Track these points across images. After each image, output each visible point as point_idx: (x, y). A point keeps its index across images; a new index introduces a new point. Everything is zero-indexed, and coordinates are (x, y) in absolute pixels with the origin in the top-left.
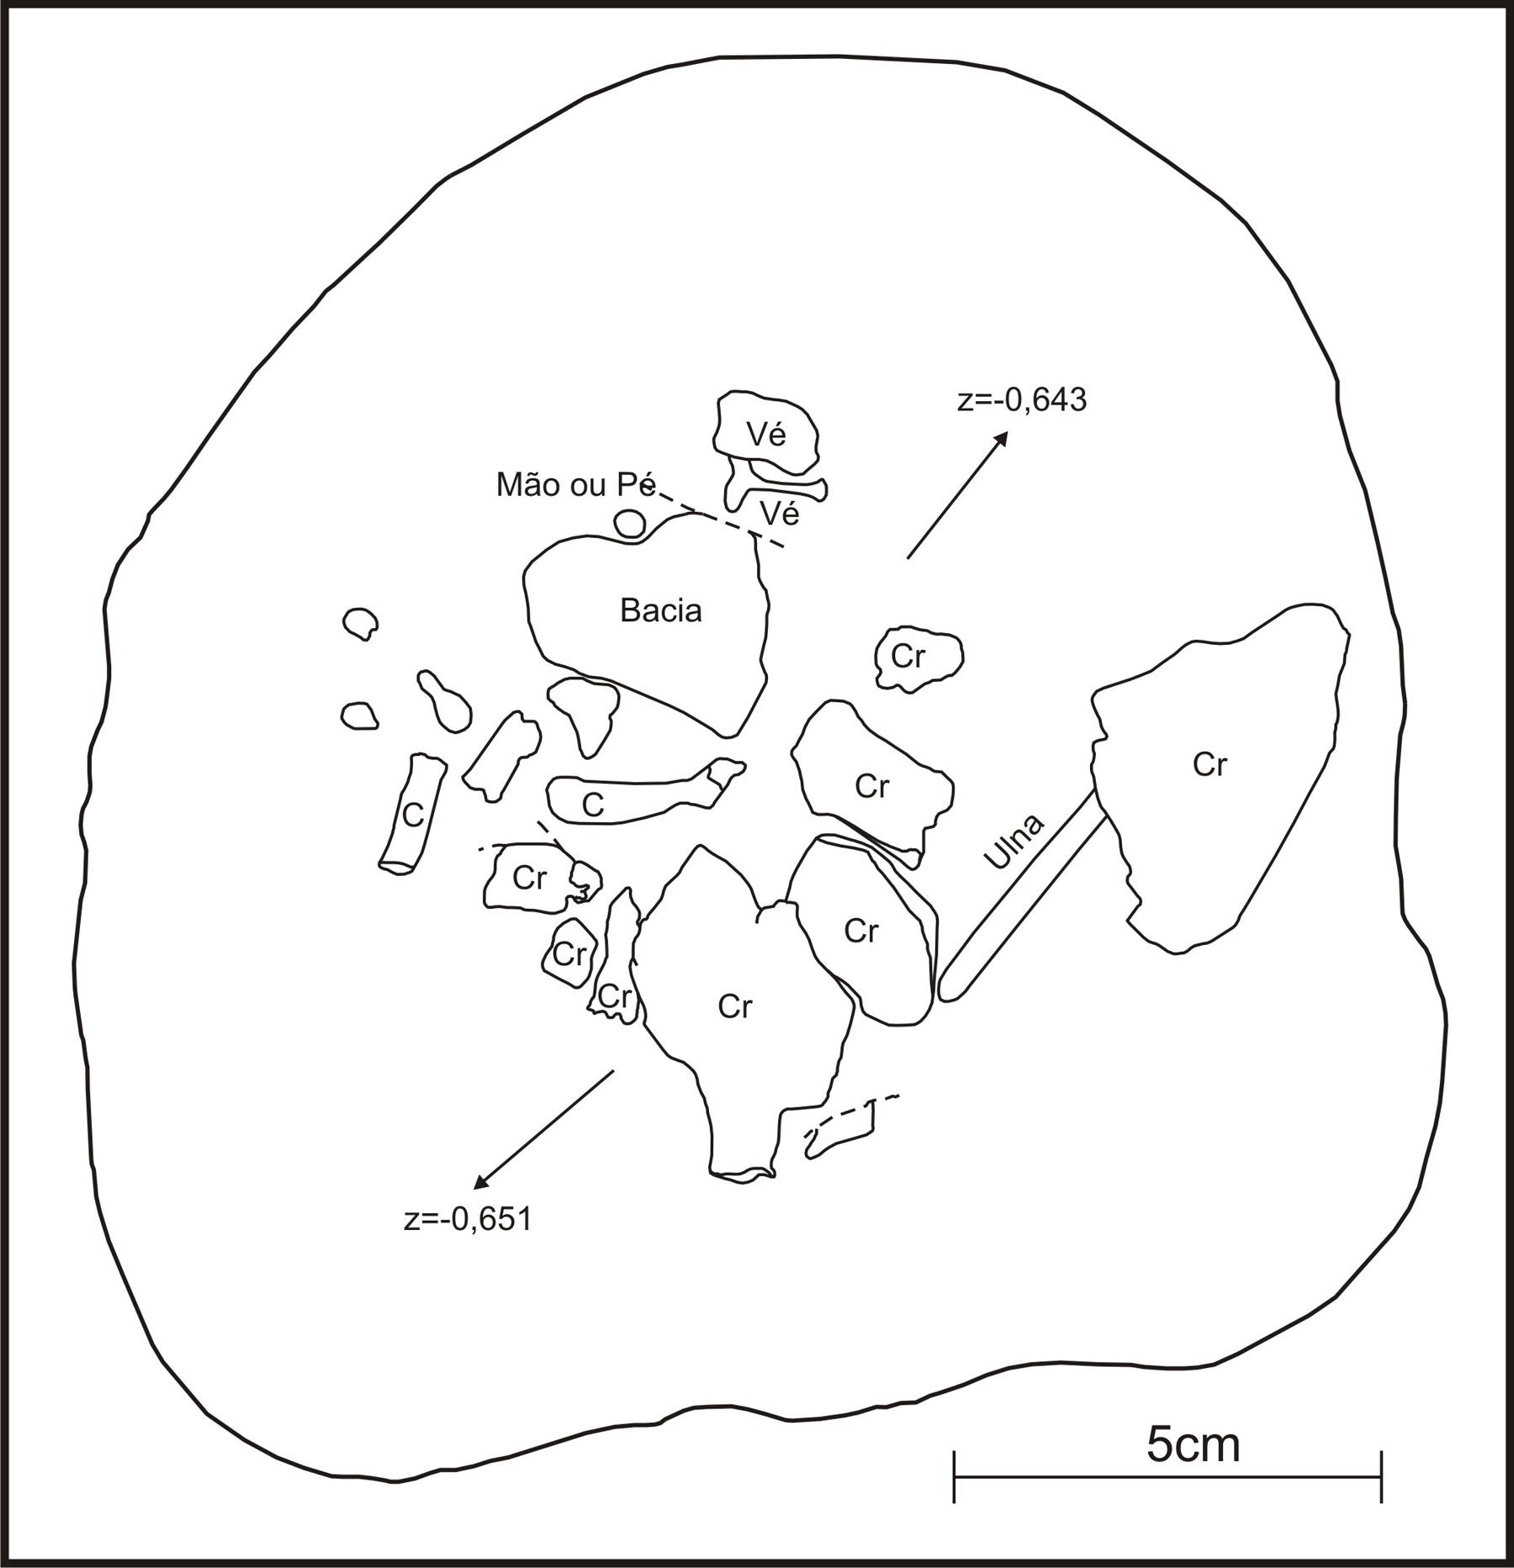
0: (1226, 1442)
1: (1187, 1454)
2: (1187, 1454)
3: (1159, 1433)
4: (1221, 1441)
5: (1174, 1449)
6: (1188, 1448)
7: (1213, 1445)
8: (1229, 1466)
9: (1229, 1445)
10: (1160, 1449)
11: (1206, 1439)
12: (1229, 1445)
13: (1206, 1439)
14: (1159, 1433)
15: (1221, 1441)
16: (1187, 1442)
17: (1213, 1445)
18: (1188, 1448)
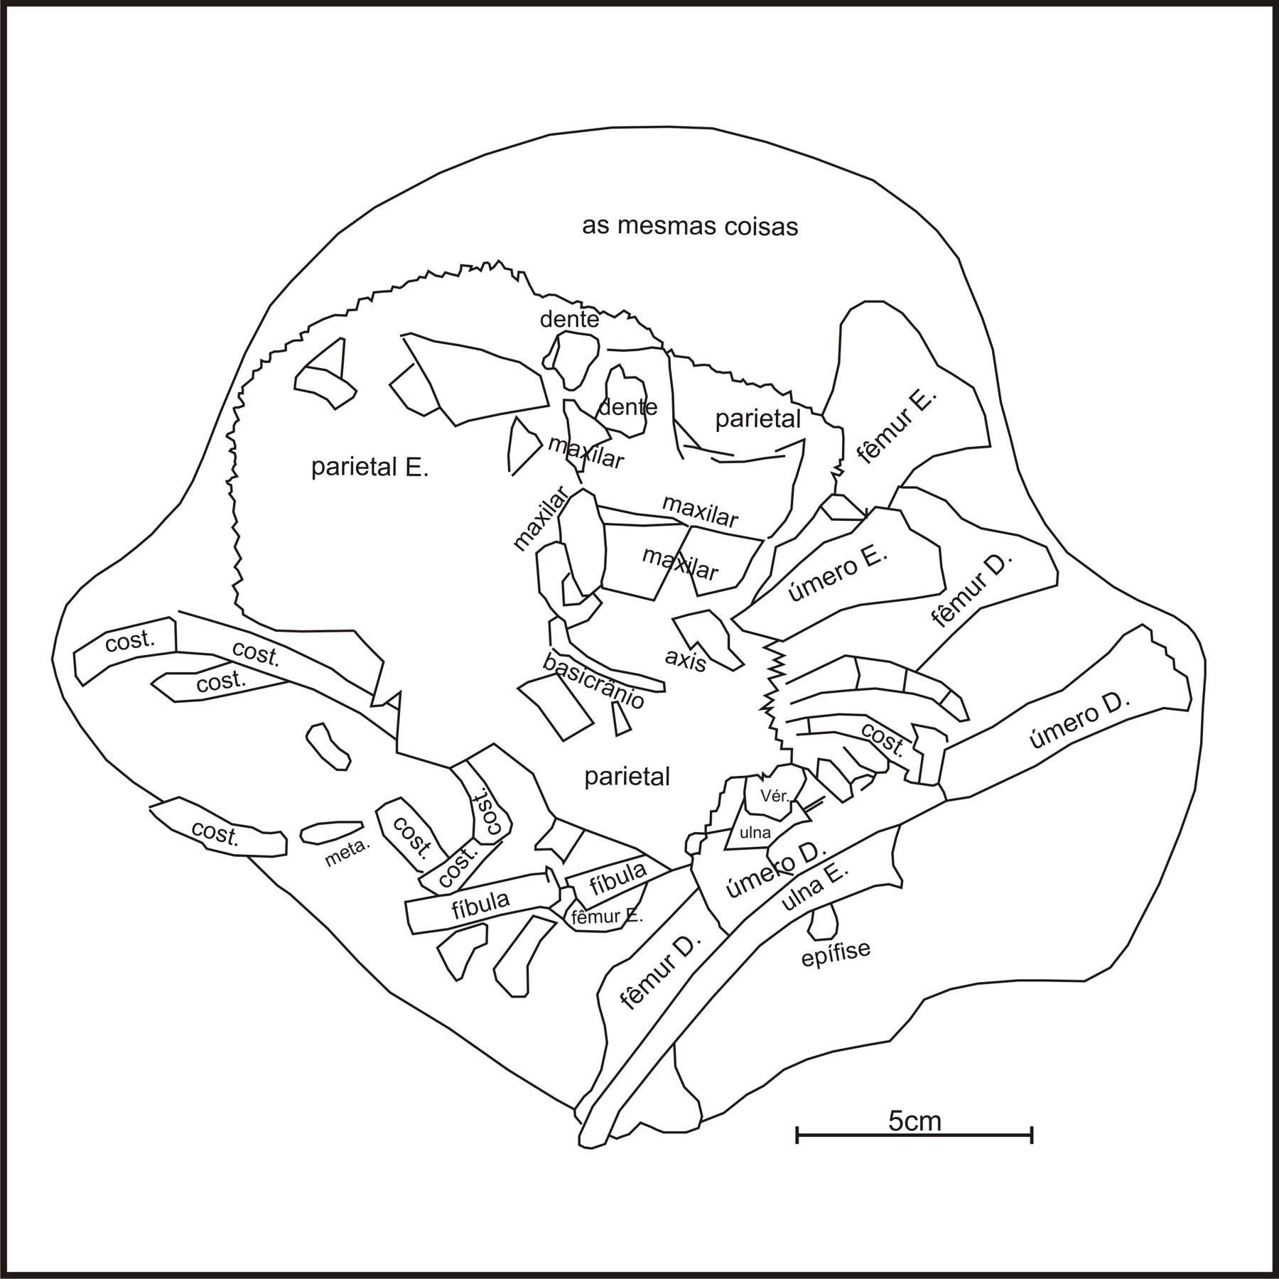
1: (911, 1125)
2: (911, 1125)
3: (895, 1115)
4: (930, 1119)
6: (912, 1123)
7: (926, 1121)
9: (935, 1121)
10: (896, 1124)
11: (922, 1118)
12: (935, 1121)
13: (922, 1118)
14: (895, 1115)
15: (930, 1119)
16: (911, 1120)
17: (926, 1121)
18: (912, 1123)
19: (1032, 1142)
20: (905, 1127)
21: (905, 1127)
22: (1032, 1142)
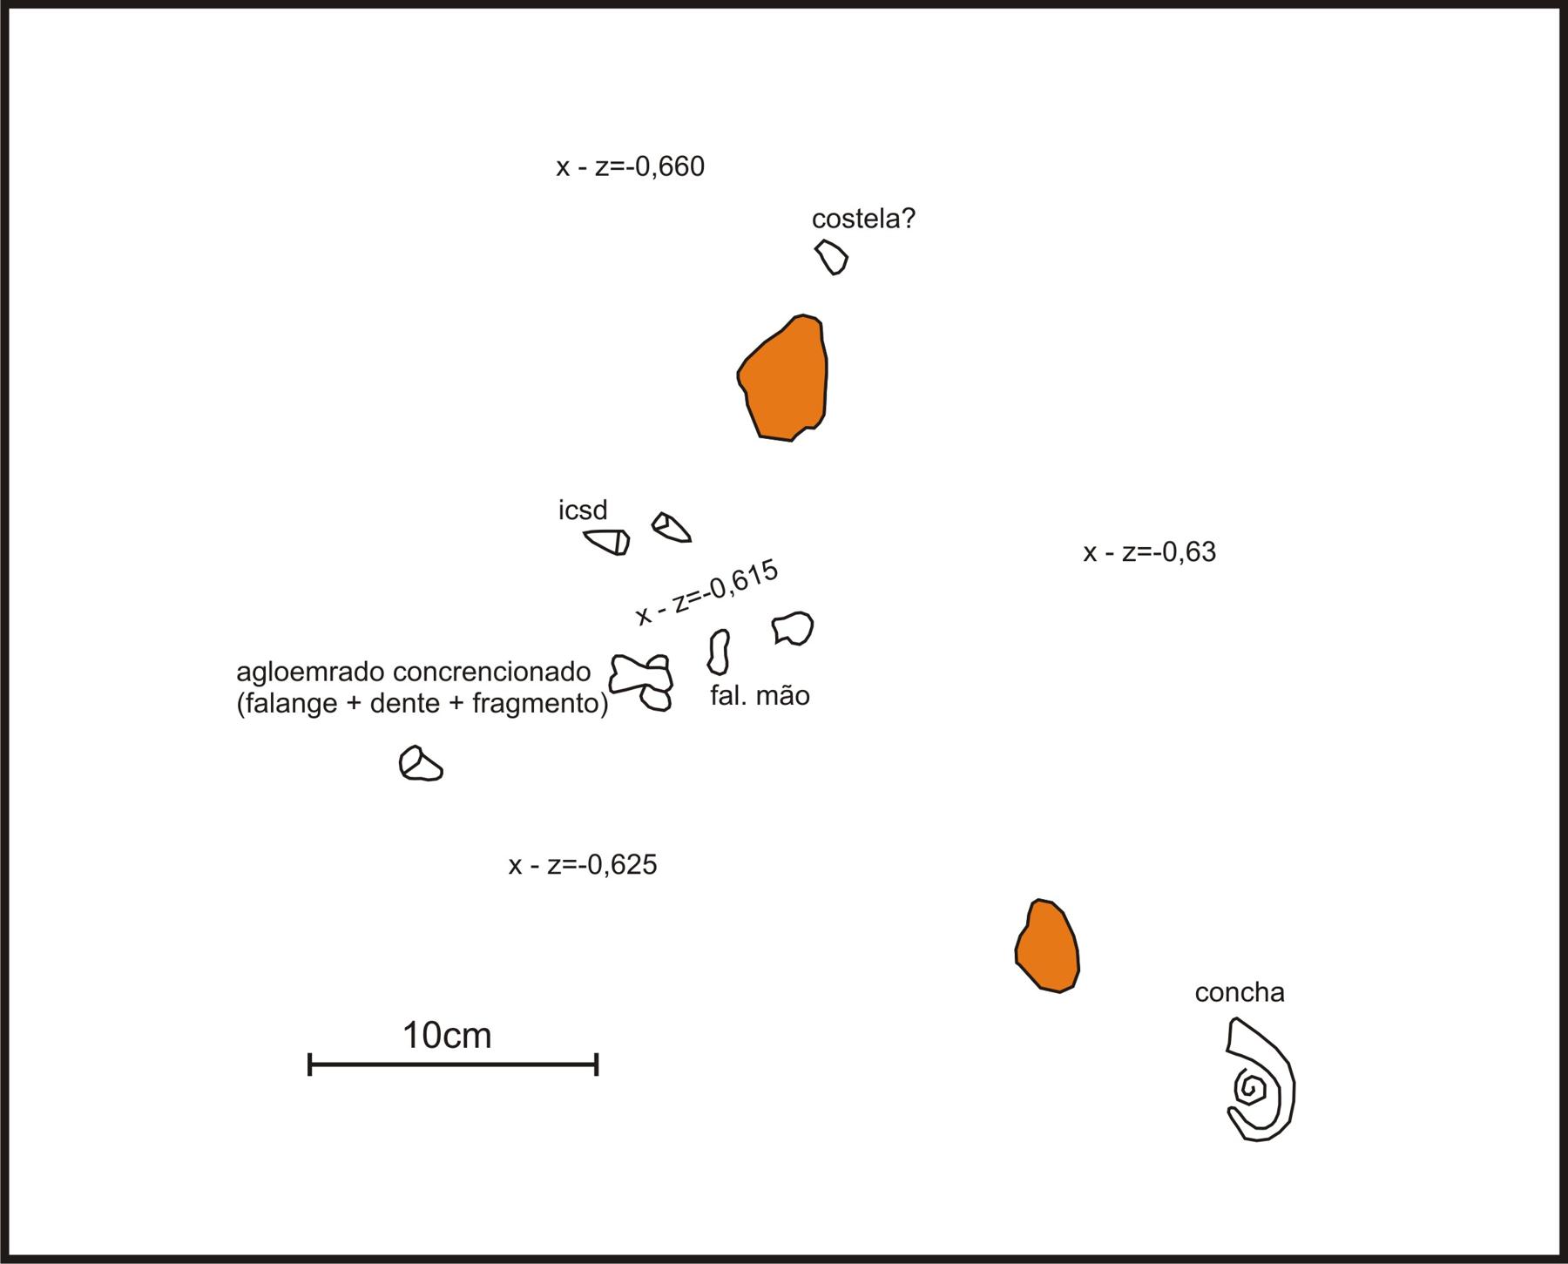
0: (481, 1034)
1: (452, 1043)
2: (452, 1043)
4: (477, 1033)
5: (442, 1037)
7: (471, 1035)
8: (482, 1055)
9: (483, 1035)
11: (466, 1032)
12: (483, 1035)
13: (466, 1032)
15: (477, 1033)
16: (452, 1035)
17: (471, 1035)
18: (453, 1038)
19: (596, 1074)
20: (447, 1045)
21: (447, 1045)
22: (596, 1074)
